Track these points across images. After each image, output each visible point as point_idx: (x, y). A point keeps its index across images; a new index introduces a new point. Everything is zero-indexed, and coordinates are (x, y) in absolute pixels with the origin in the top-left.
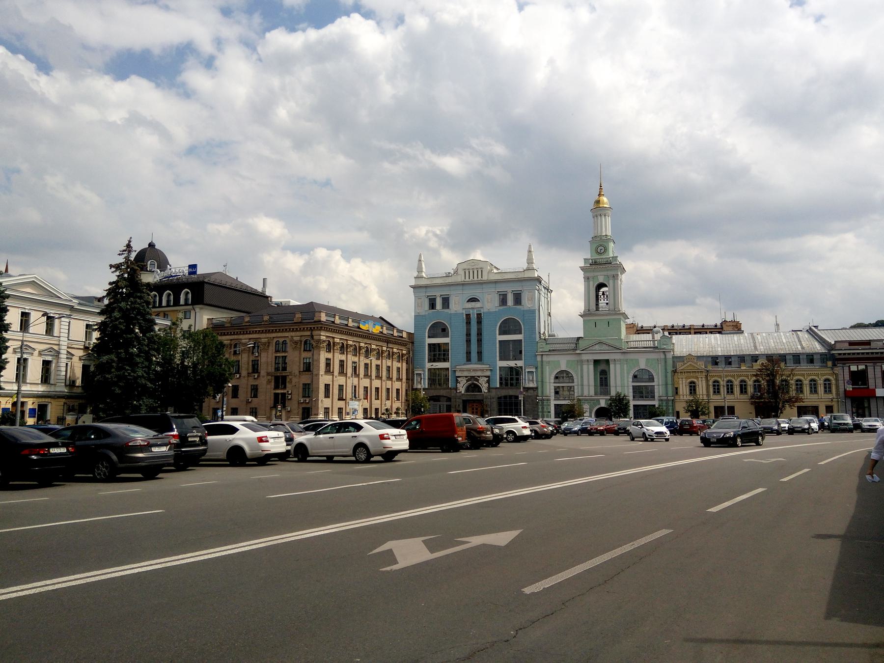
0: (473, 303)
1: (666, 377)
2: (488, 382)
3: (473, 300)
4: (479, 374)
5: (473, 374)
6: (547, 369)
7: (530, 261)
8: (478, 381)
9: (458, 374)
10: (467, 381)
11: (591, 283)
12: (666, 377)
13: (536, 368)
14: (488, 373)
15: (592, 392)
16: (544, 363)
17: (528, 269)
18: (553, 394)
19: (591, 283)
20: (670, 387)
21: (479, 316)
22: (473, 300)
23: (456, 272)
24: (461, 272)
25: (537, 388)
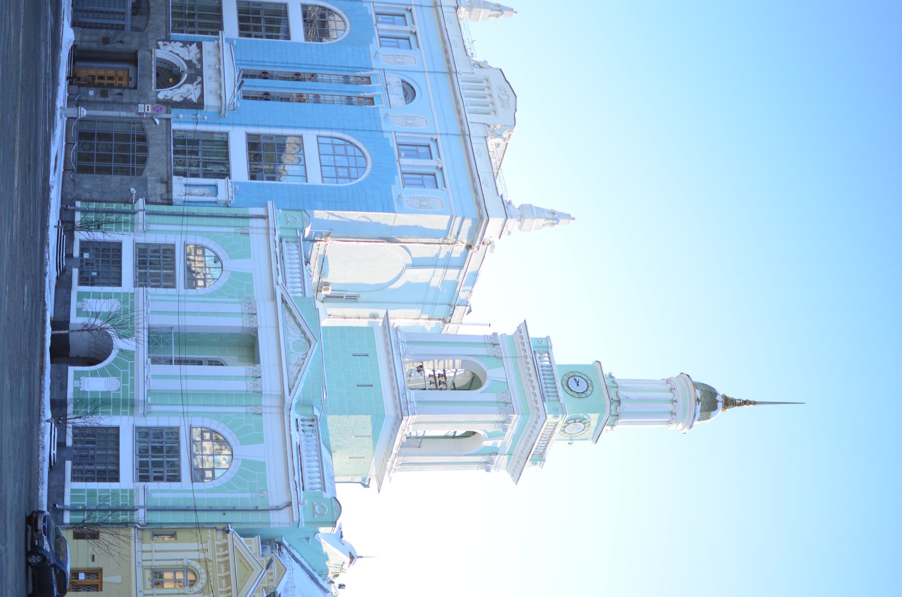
0: (400, 90)
1: (210, 510)
2: (186, 104)
3: (409, 92)
4: (209, 84)
5: (208, 72)
6: (226, 228)
7: (528, 212)
8: (190, 80)
9: (208, 46)
10: (189, 63)
11: (483, 351)
12: (210, 510)
13: (227, 205)
14: (210, 101)
15: (158, 321)
16: (241, 222)
17: (506, 205)
18: (150, 239)
19: (483, 351)
20: (181, 517)
21: (371, 101)
22: (409, 92)
23: (480, 66)
24: (479, 73)
25: (170, 202)
